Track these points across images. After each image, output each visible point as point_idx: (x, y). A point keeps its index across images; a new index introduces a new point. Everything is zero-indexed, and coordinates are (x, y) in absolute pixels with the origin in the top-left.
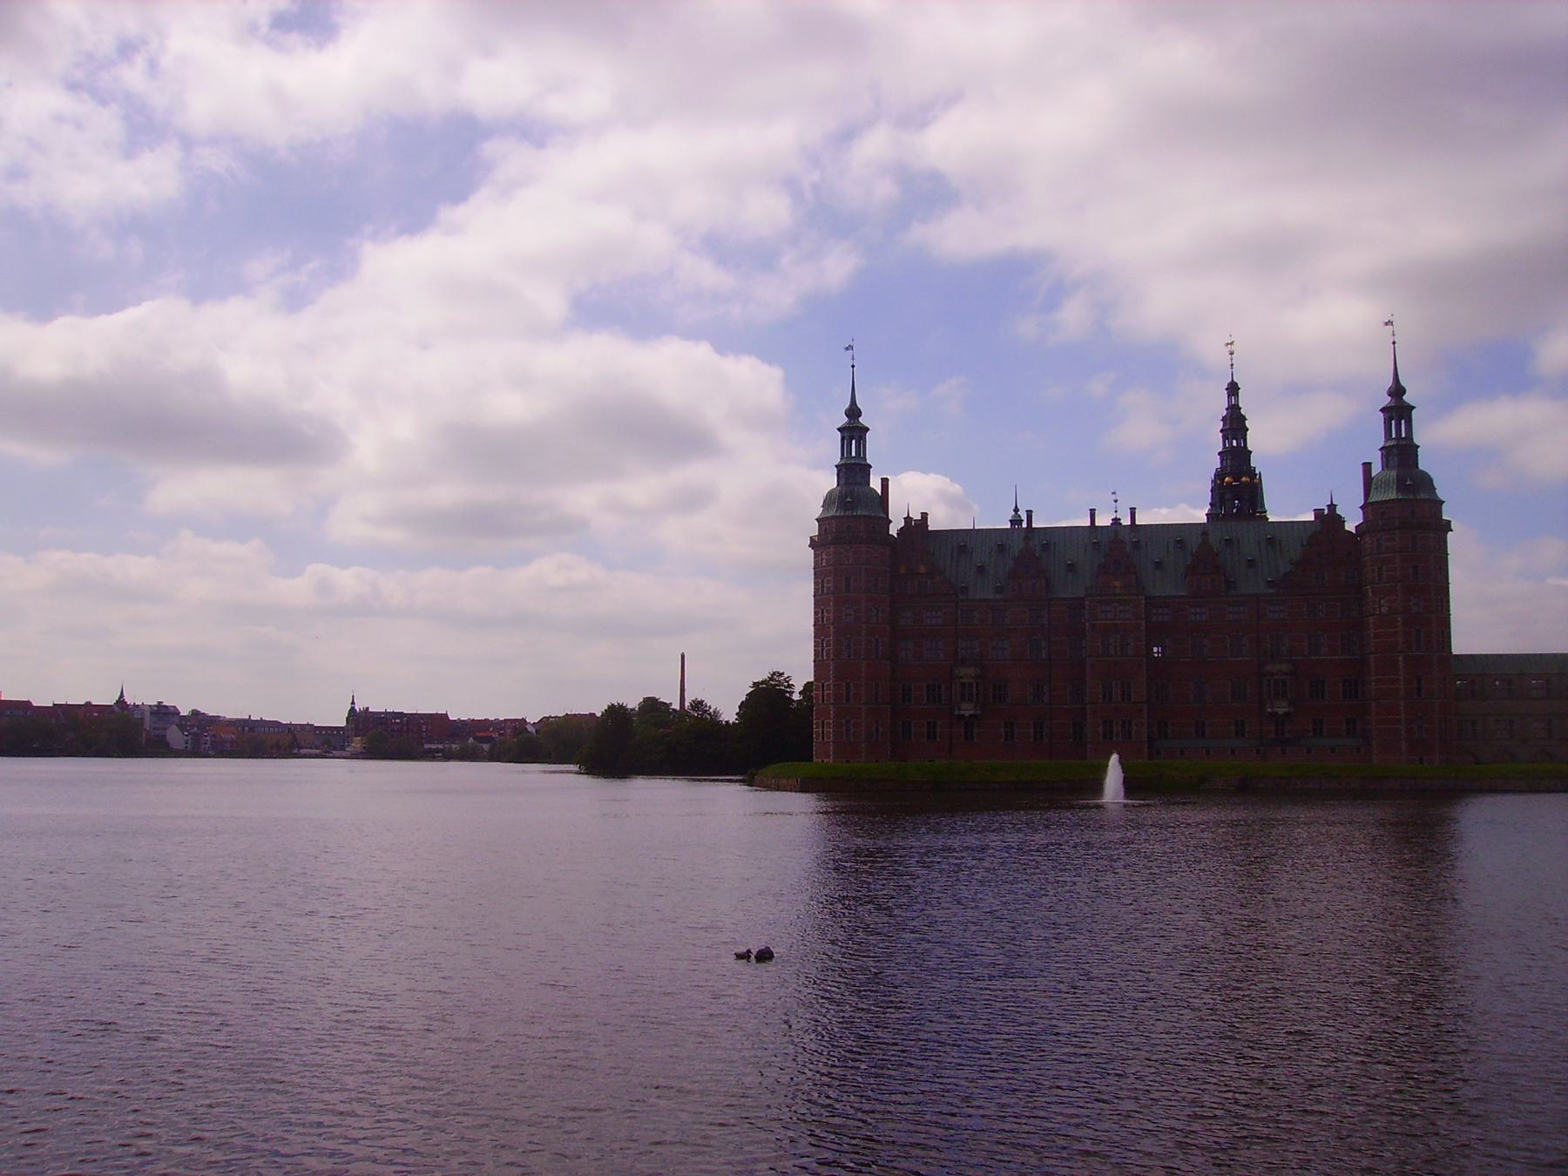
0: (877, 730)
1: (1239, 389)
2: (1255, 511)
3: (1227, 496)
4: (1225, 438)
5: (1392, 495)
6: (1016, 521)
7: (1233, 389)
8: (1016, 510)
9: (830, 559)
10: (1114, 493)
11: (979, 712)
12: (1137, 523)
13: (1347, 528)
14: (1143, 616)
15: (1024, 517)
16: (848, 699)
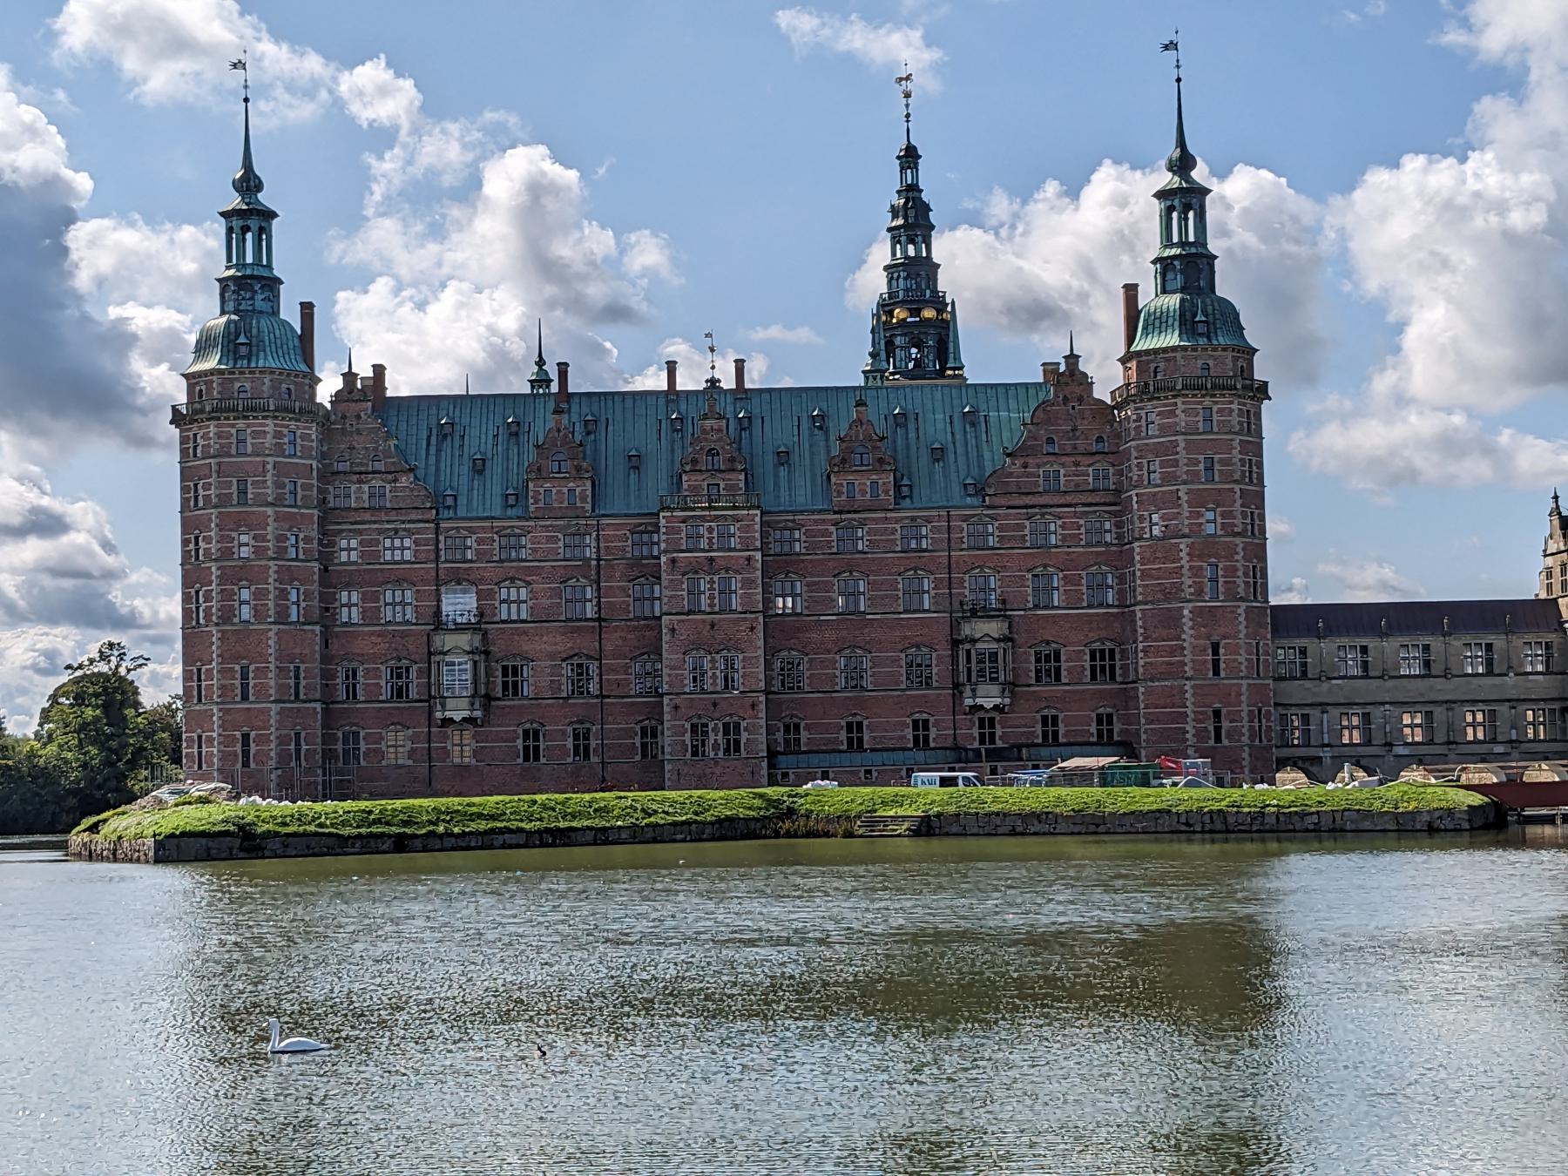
0: (298, 751)
1: (920, 157)
2: (943, 368)
3: (898, 341)
4: (895, 241)
5: (1172, 339)
6: (541, 381)
7: (910, 157)
8: (541, 362)
9: (209, 446)
10: (708, 335)
11: (478, 714)
12: (748, 385)
13: (1096, 395)
14: (758, 544)
15: (554, 375)
16: (245, 698)
